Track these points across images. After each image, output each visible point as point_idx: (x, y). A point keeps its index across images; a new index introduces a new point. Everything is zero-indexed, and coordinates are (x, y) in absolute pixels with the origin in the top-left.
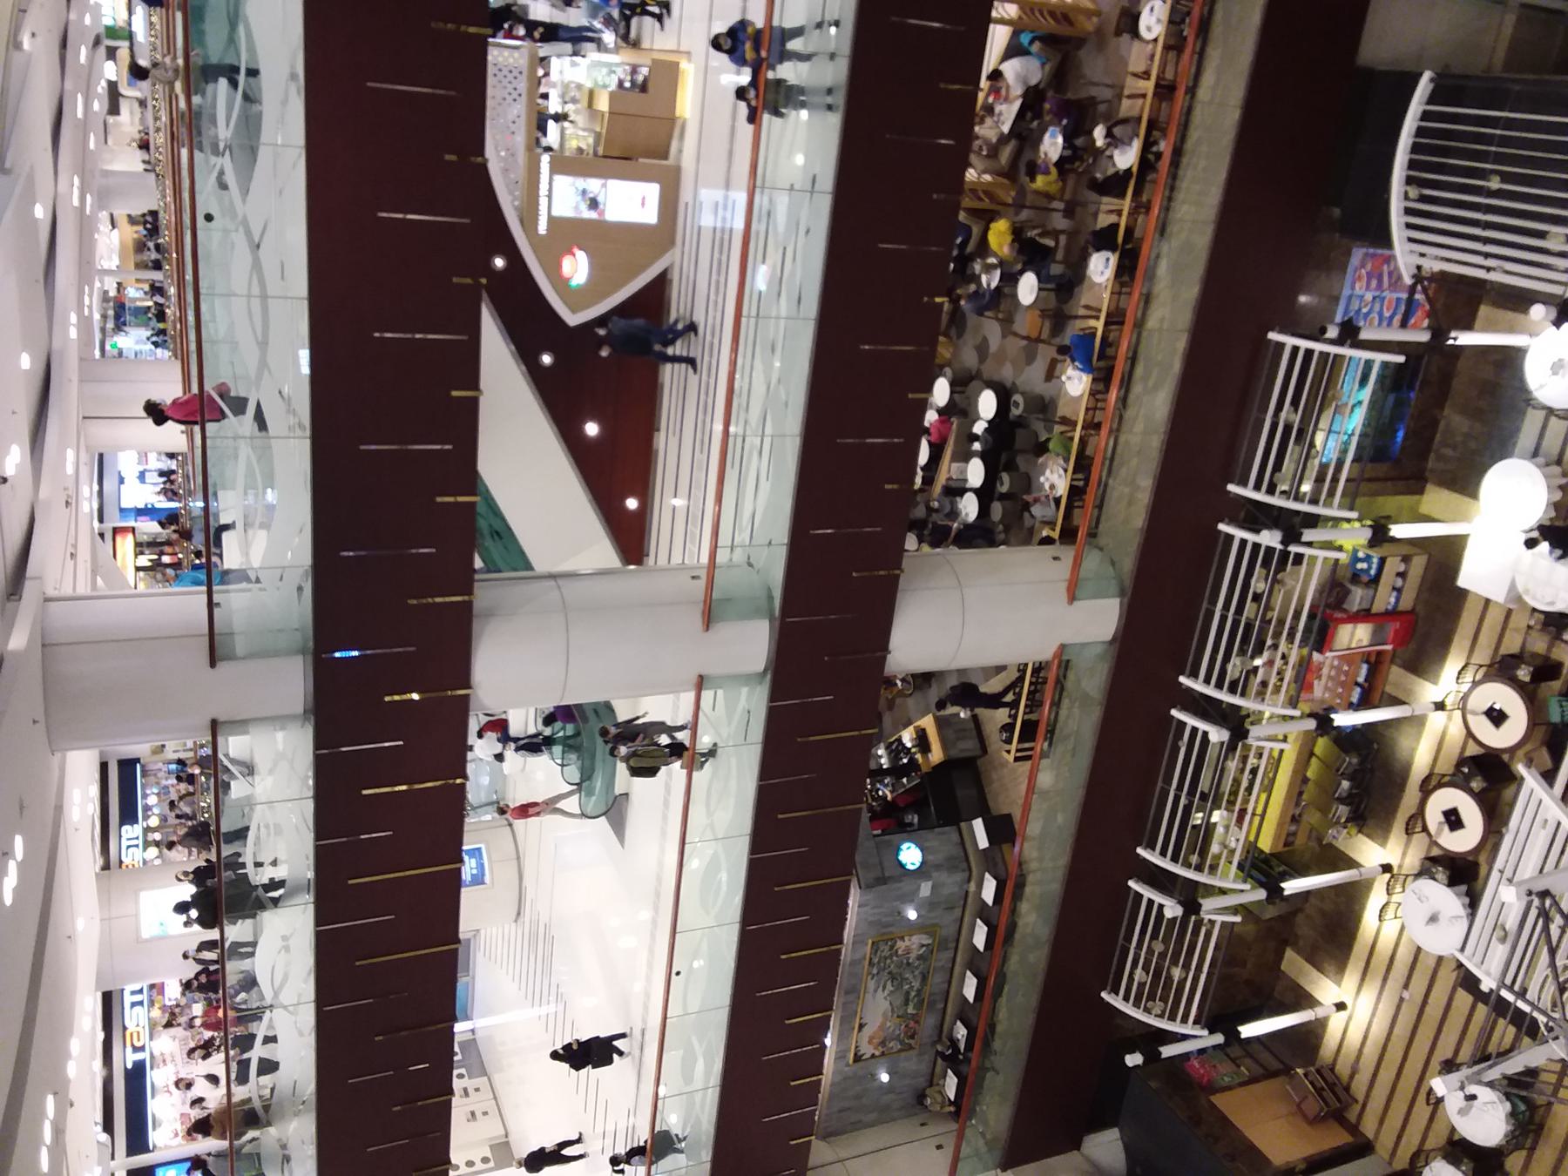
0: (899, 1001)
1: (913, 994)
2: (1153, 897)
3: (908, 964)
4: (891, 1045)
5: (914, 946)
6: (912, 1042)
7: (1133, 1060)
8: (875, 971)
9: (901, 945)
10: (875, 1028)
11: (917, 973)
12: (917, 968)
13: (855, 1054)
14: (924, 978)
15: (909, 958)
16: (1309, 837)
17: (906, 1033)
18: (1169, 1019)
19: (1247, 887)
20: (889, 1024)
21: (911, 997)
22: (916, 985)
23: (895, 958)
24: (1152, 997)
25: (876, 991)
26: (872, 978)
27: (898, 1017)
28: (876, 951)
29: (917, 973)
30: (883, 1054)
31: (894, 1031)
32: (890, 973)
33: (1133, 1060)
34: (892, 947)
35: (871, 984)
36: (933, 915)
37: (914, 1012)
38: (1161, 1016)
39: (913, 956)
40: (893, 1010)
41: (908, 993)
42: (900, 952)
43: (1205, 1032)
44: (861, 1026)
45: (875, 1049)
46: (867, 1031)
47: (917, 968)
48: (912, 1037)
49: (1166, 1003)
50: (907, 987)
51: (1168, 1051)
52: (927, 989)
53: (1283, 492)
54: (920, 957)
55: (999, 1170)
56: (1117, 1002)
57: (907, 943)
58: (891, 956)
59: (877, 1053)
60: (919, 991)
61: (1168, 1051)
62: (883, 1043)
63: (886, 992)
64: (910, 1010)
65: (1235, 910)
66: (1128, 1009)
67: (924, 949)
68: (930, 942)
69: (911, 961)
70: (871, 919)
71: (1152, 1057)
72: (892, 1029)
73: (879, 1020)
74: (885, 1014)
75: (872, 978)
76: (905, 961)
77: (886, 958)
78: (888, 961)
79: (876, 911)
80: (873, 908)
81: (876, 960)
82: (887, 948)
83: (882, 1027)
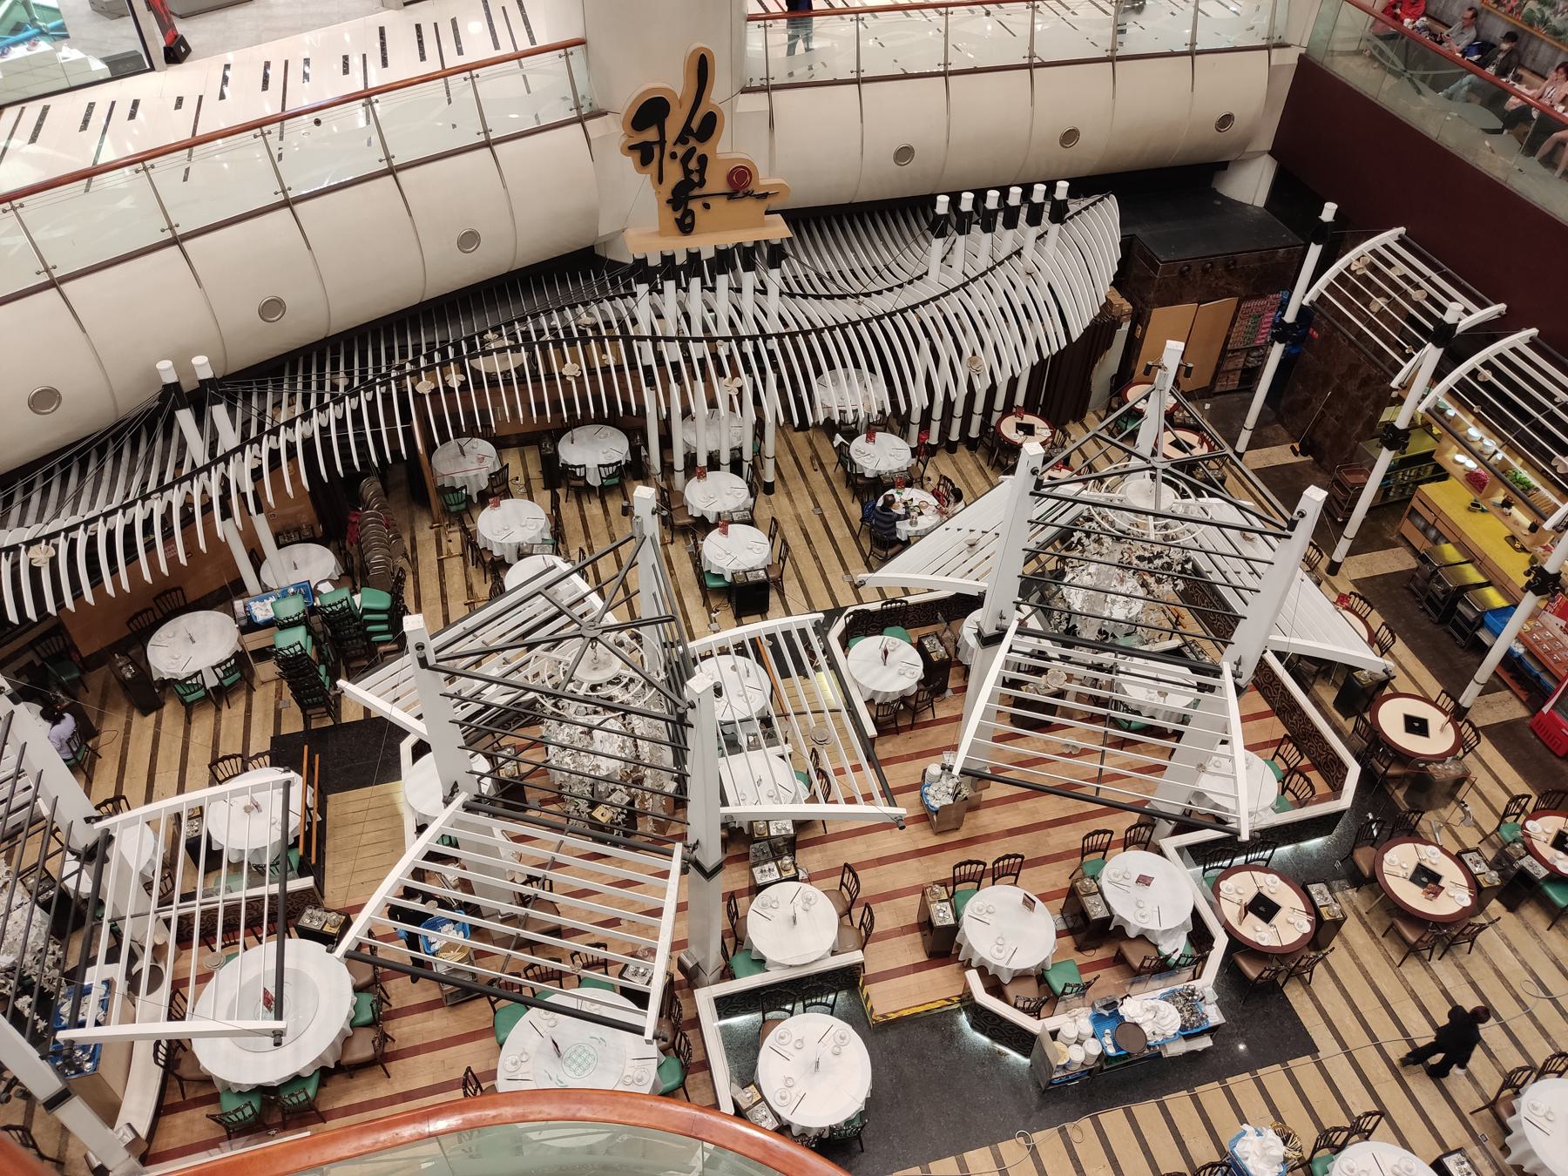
1: (1548, 12)
2: (1472, 318)
7: (1329, 212)
14: (1556, 33)
16: (1403, 537)
18: (1341, 274)
19: (1421, 409)
24: (1373, 268)
33: (1329, 212)
38: (1348, 269)
43: (1305, 302)
49: (1359, 278)
50: (1561, 7)
51: (1314, 251)
52: (1542, 32)
55: (1303, 51)
56: (1390, 236)
60: (1544, 22)
61: (1314, 251)
65: (1405, 387)
66: (1375, 242)
71: (1317, 231)
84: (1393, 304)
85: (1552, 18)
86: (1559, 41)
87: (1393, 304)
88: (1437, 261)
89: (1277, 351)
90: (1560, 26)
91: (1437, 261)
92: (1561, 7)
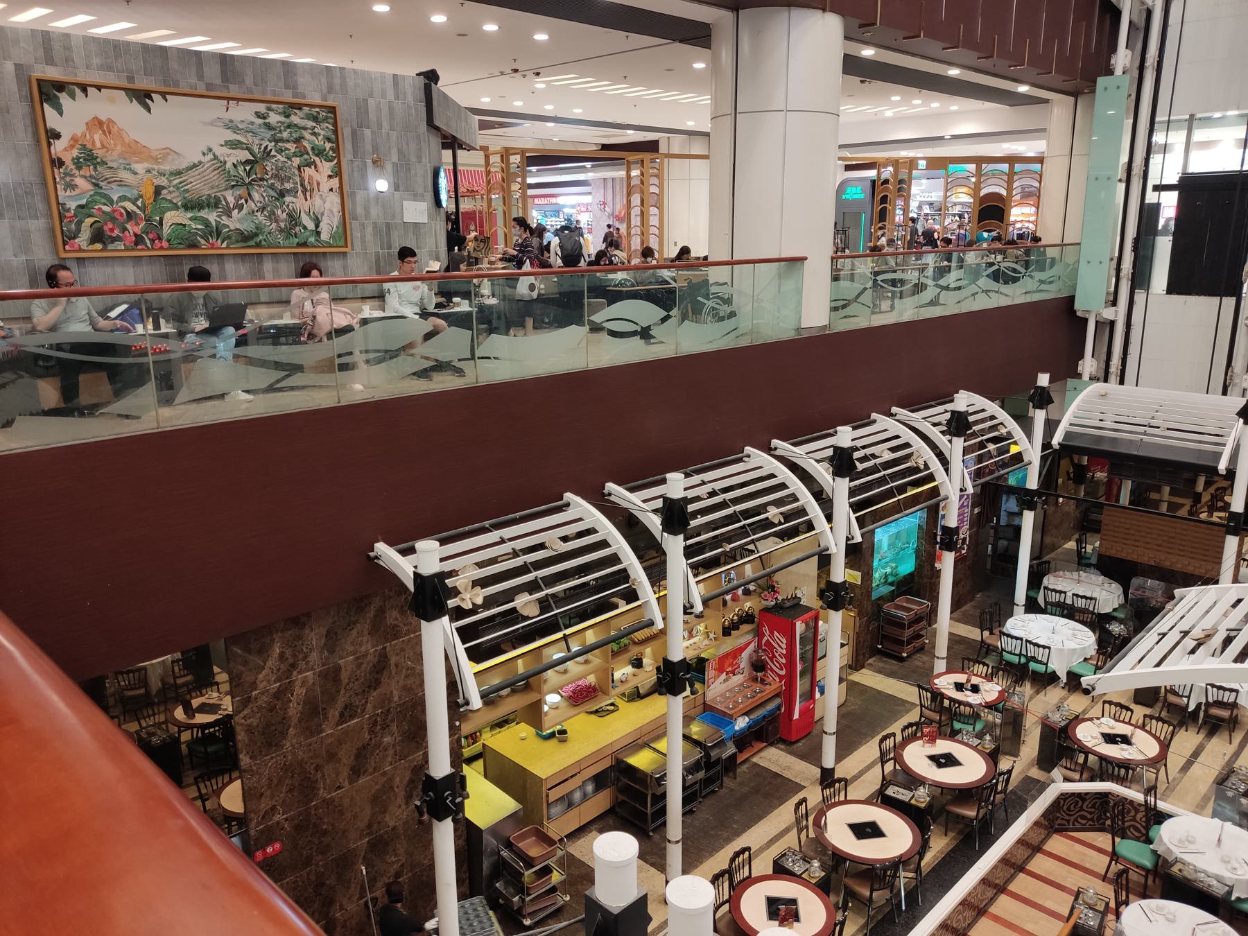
0: (200, 186)
1: (212, 217)
3: (282, 194)
4: (79, 181)
5: (317, 201)
6: (83, 240)
8: (274, 118)
9: (326, 167)
10: (134, 134)
11: (261, 218)
12: (272, 217)
13: (61, 86)
14: (245, 237)
15: (295, 195)
17: (111, 217)
20: (140, 168)
21: (203, 214)
22: (236, 222)
23: (297, 161)
25: (230, 125)
26: (258, 115)
27: (158, 190)
28: (315, 119)
29: (261, 218)
30: (58, 163)
31: (121, 183)
32: (267, 154)
34: (320, 152)
35: (244, 113)
36: (369, 230)
37: (166, 230)
39: (297, 202)
40: (178, 173)
41: (213, 203)
42: (309, 171)
44: (143, 97)
45: (74, 139)
46: (124, 112)
47: (272, 217)
48: (98, 236)
50: (231, 200)
53: (463, 907)
54: (294, 219)
57: (325, 186)
58: (302, 153)
59: (59, 147)
62: (88, 158)
63: (221, 151)
64: (172, 218)
67: (311, 226)
68: (325, 236)
69: (288, 199)
70: (372, 103)
72: (125, 175)
73: (153, 142)
74: (167, 152)
75: (258, 115)
76: (288, 186)
77: (298, 141)
78: (292, 147)
79: (385, 110)
80: (391, 109)
81: (295, 119)
82: (319, 142)
83: (135, 150)
84: (532, 587)
85: (225, 220)
86: (258, 245)
87: (532, 587)
88: (467, 528)
89: (1028, 519)
90: (247, 226)
91: (467, 528)
92: (231, 200)
